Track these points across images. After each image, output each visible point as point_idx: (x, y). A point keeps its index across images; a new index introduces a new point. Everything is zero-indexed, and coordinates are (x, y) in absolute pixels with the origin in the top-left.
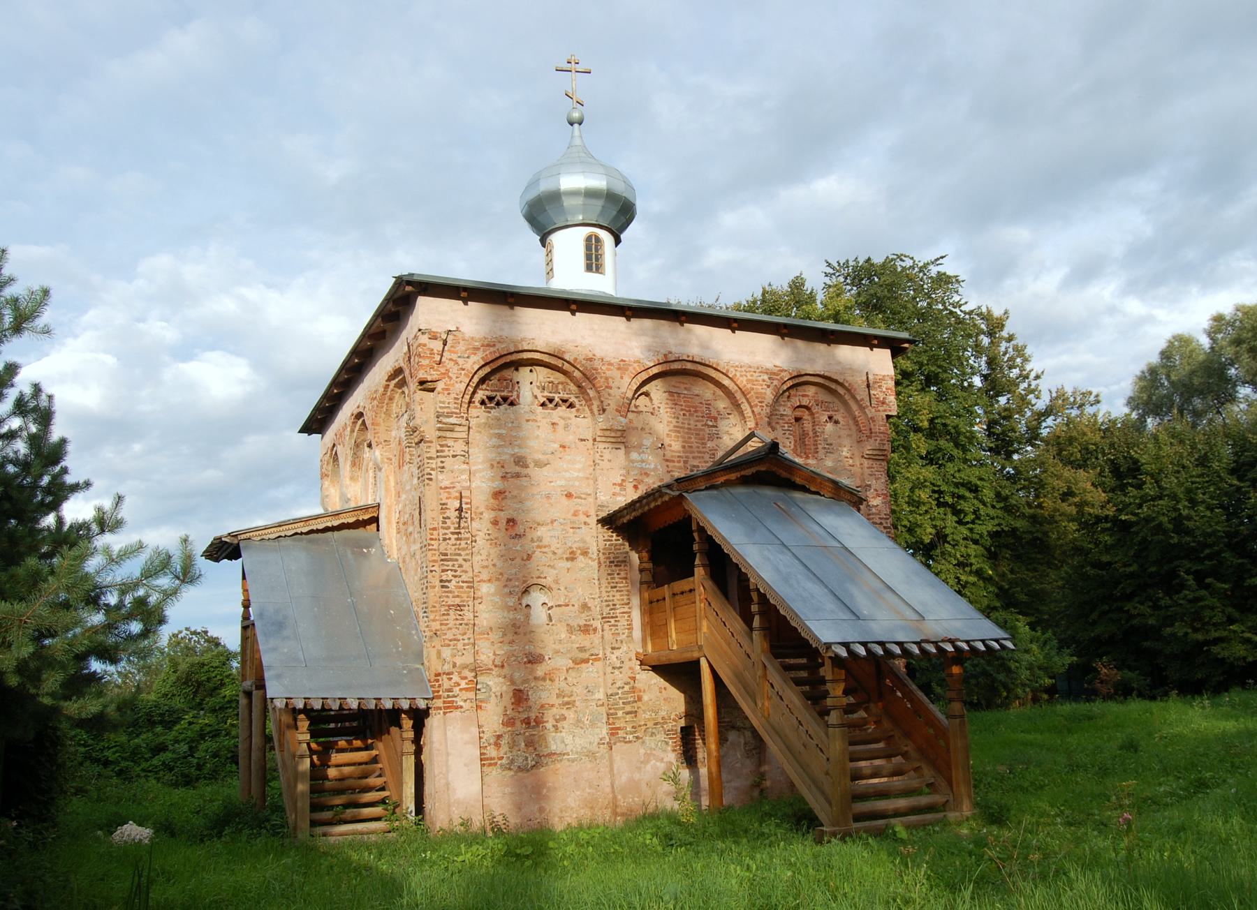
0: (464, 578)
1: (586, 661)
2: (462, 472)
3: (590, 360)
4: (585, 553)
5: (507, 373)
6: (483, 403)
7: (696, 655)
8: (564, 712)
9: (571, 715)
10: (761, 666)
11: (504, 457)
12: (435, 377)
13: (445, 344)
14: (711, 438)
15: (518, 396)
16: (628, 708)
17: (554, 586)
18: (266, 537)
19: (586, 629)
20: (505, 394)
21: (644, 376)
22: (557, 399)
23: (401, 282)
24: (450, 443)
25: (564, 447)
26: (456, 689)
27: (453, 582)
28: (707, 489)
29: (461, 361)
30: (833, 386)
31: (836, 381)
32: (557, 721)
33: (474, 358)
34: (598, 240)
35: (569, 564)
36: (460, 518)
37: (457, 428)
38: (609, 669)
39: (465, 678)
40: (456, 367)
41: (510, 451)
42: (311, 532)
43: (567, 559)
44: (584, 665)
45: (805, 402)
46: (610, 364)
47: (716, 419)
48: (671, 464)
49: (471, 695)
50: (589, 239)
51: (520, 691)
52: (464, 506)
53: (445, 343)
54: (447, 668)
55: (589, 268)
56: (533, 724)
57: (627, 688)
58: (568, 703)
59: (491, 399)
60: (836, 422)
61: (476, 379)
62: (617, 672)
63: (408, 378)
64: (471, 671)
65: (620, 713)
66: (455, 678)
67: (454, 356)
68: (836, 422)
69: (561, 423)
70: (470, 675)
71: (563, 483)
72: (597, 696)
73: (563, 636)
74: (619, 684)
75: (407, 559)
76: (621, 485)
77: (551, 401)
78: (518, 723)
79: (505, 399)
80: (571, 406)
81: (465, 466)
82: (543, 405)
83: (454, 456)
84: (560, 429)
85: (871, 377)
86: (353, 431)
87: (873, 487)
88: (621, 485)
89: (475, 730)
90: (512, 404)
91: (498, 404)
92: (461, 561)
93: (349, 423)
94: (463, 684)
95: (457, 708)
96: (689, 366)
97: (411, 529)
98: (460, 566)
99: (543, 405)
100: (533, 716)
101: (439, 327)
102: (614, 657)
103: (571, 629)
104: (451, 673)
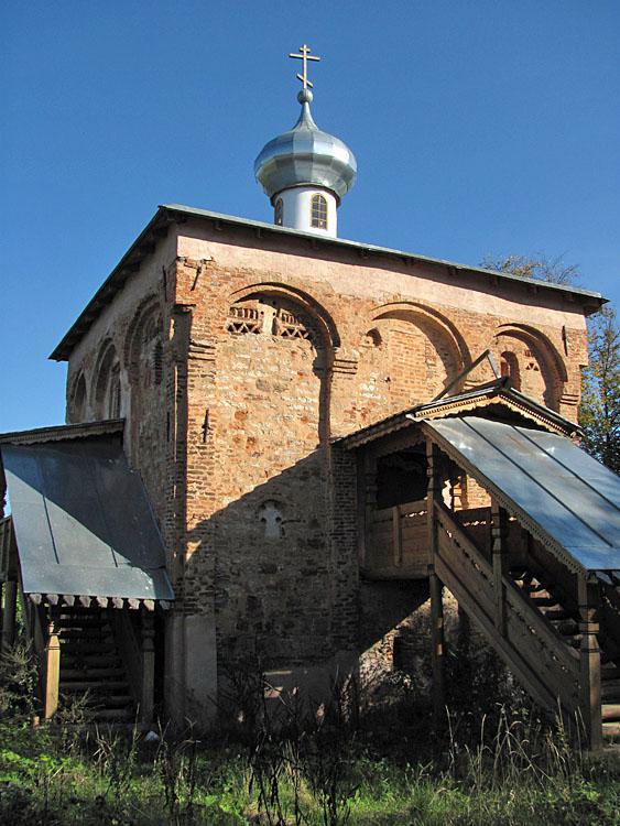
0: (208, 490)
1: (315, 573)
2: (208, 391)
3: (329, 296)
4: (316, 474)
6: (230, 329)
7: (425, 573)
8: (293, 619)
9: (299, 623)
10: (500, 585)
11: (249, 380)
12: (189, 302)
13: (199, 271)
14: (429, 376)
16: (350, 619)
17: (288, 502)
18: (24, 442)
19: (315, 544)
20: (250, 322)
22: (296, 331)
23: (164, 213)
24: (200, 363)
25: (301, 374)
26: (198, 593)
27: (198, 493)
28: (446, 417)
29: (213, 288)
32: (286, 627)
34: (324, 201)
35: (302, 483)
36: (205, 433)
37: (207, 351)
38: (334, 583)
39: (206, 584)
40: (209, 293)
41: (251, 374)
42: (64, 440)
43: (301, 479)
44: (312, 578)
45: (510, 349)
49: (210, 599)
50: (315, 199)
51: (253, 598)
52: (210, 423)
53: (199, 271)
54: (188, 573)
55: (315, 224)
56: (264, 629)
57: (350, 600)
58: (297, 611)
59: (238, 326)
62: (342, 585)
63: (163, 303)
64: (211, 577)
65: (344, 623)
66: (196, 583)
67: (208, 284)
69: (300, 352)
70: (210, 581)
71: (301, 407)
72: (322, 606)
73: (294, 549)
74: (344, 596)
75: (150, 470)
76: (351, 413)
77: (291, 331)
78: (251, 628)
79: (250, 327)
81: (210, 386)
82: (284, 334)
83: (203, 376)
84: (298, 357)
85: (567, 330)
86: (100, 356)
88: (351, 413)
89: (213, 632)
90: (256, 332)
91: (244, 331)
92: (205, 475)
93: (98, 348)
94: (203, 590)
95: (197, 611)
97: (155, 443)
98: (205, 479)
99: (284, 334)
100: (264, 622)
101: (196, 257)
102: (340, 571)
103: (301, 543)
104: (194, 578)
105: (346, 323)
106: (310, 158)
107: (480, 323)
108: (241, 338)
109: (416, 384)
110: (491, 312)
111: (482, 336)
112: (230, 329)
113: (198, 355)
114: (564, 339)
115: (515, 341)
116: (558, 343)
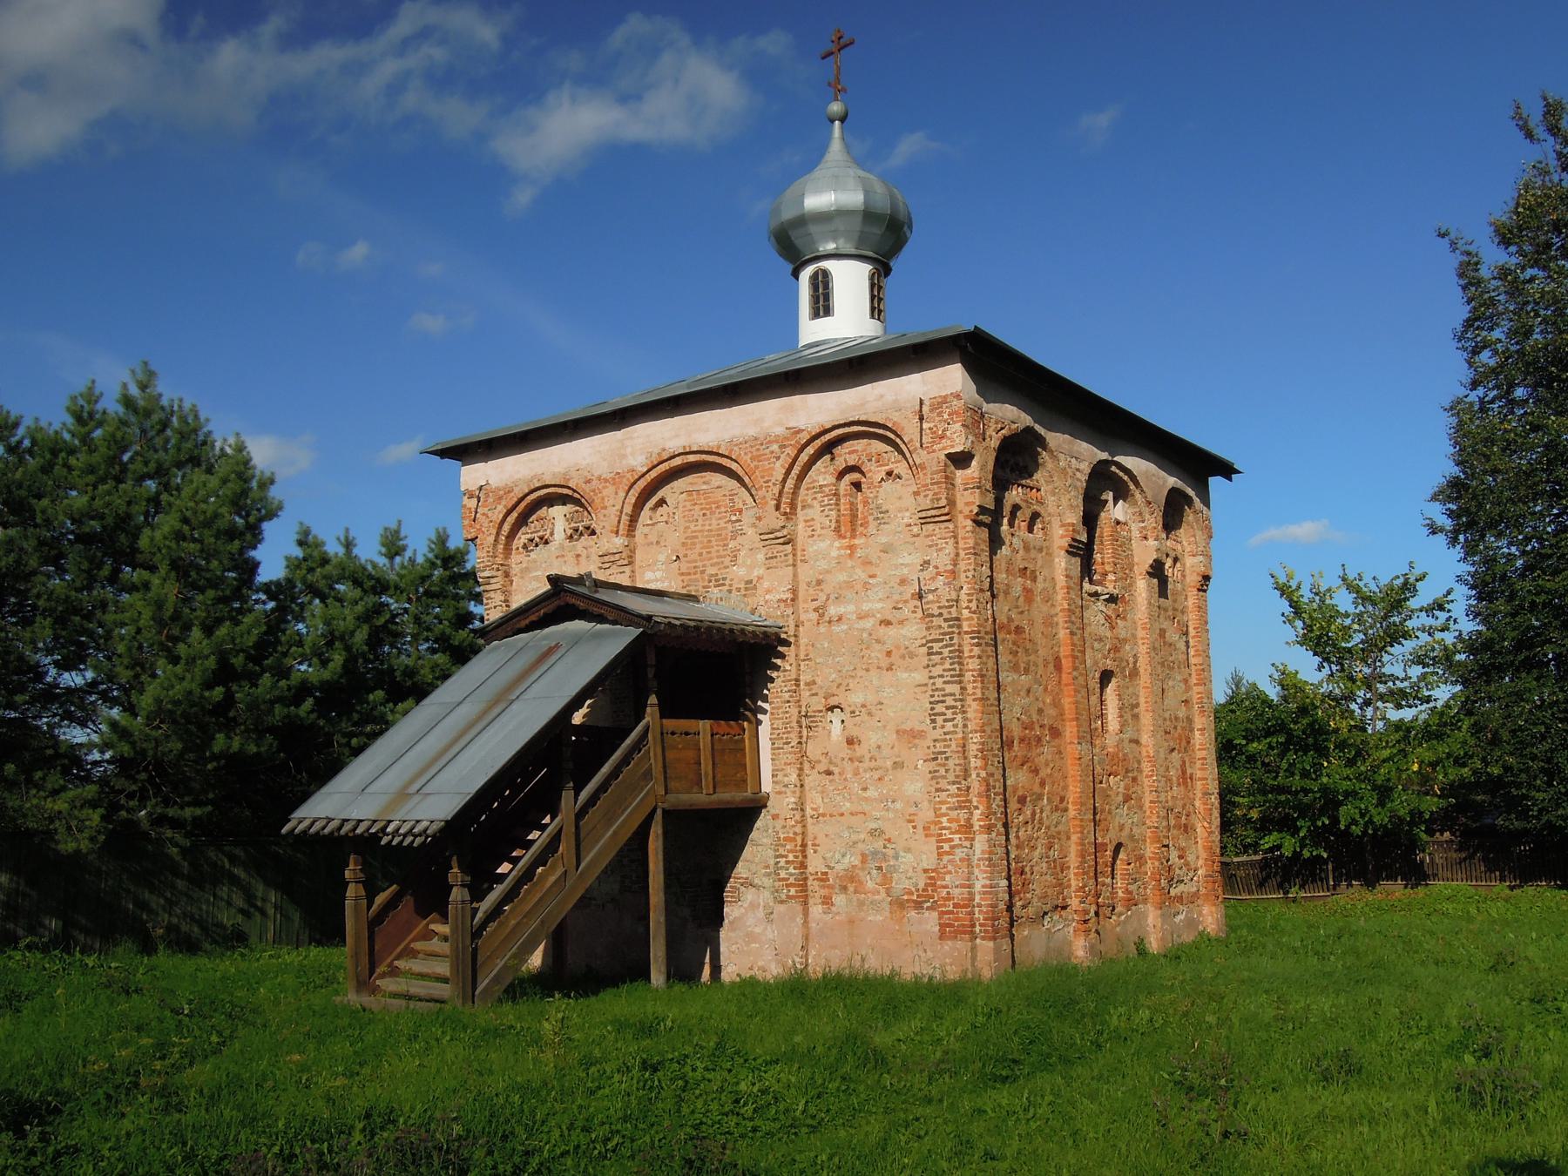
3: (588, 481)
5: (543, 512)
14: (734, 538)
15: (552, 534)
21: (642, 484)
24: (492, 594)
33: (500, 507)
46: (606, 481)
47: (741, 511)
48: (686, 578)
50: (814, 277)
61: (506, 527)
77: (576, 530)
79: (541, 538)
80: (593, 533)
82: (571, 537)
84: (583, 559)
85: (927, 403)
87: (933, 563)
90: (546, 542)
96: (692, 458)
101: (473, 487)
105: (605, 508)
106: (803, 221)
107: (775, 447)
109: (714, 554)
111: (778, 464)
112: (525, 547)
113: (488, 587)
114: (921, 419)
115: (860, 444)
116: (910, 431)
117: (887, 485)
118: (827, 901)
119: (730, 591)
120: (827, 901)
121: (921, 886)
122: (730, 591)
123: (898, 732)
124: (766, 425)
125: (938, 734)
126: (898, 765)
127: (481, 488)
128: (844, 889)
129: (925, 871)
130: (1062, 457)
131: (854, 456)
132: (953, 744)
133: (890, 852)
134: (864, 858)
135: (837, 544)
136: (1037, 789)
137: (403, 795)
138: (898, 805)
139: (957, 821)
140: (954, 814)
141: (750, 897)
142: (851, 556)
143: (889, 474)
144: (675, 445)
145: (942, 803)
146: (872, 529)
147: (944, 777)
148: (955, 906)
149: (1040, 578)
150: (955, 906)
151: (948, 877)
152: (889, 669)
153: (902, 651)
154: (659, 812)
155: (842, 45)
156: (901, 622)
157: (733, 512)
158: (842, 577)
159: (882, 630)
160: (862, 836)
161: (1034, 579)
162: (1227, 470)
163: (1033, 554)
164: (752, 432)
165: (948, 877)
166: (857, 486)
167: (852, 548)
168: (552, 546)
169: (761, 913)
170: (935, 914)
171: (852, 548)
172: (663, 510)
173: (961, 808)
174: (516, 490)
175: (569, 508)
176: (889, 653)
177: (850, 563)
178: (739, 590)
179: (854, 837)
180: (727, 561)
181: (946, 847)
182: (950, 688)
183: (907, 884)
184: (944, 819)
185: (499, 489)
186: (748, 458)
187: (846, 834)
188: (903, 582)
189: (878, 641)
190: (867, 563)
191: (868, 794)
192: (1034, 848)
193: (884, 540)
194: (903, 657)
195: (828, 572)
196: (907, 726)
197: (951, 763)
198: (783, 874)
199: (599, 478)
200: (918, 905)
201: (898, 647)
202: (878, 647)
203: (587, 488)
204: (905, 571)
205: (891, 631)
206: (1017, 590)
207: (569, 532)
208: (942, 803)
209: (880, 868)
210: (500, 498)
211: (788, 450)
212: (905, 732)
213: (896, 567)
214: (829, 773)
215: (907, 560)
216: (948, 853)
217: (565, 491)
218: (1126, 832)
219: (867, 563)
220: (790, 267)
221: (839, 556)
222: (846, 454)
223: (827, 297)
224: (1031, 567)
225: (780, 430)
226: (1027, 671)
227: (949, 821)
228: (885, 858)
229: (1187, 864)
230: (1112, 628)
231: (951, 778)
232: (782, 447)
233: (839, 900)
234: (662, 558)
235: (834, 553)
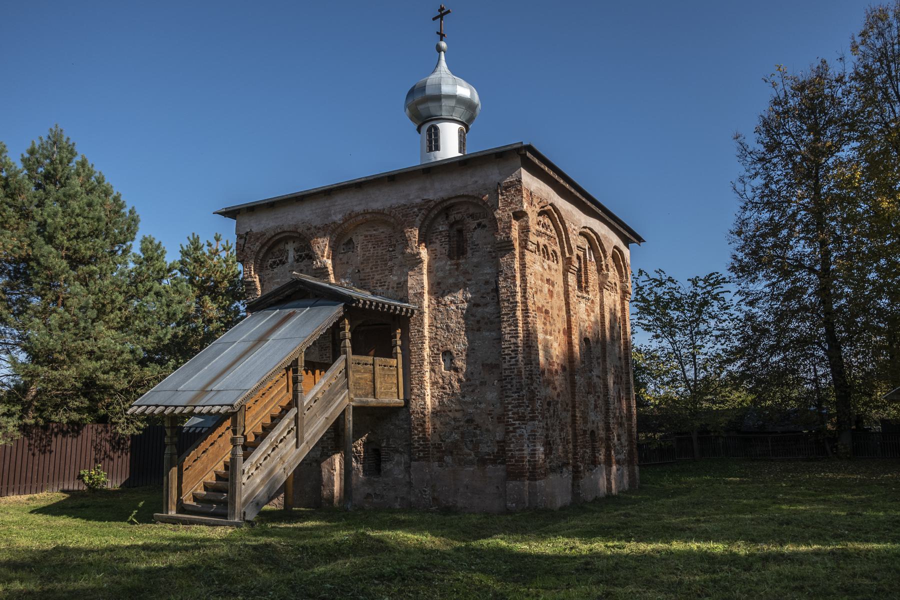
3: (309, 229)
5: (281, 246)
14: (391, 260)
15: (287, 258)
30: (475, 201)
31: (474, 197)
33: (257, 244)
45: (458, 217)
46: (319, 228)
47: (395, 246)
50: (429, 130)
59: (274, 262)
60: (484, 226)
61: (261, 255)
68: (484, 226)
77: (300, 256)
79: (280, 261)
90: (284, 263)
99: (297, 261)
107: (416, 209)
108: (275, 270)
110: (425, 197)
112: (271, 266)
117: (478, 231)
118: (441, 459)
119: (388, 289)
120: (441, 459)
121: (496, 450)
122: (388, 289)
123: (483, 365)
124: (411, 197)
125: (505, 366)
126: (483, 383)
127: (247, 233)
128: (451, 453)
129: (498, 442)
130: (566, 222)
131: (459, 215)
132: (516, 371)
133: (478, 432)
134: (463, 434)
135: (449, 263)
136: (556, 398)
137: (204, 391)
138: (483, 406)
139: (518, 413)
140: (515, 410)
141: (396, 459)
142: (457, 269)
143: (479, 225)
144: (358, 209)
145: (509, 403)
146: (469, 254)
147: (510, 389)
148: (516, 461)
149: (556, 286)
150: (516, 461)
151: (512, 445)
152: (479, 330)
153: (486, 320)
154: (351, 408)
155: (442, 14)
156: (486, 305)
157: (391, 246)
158: (451, 281)
159: (474, 309)
160: (462, 423)
161: (553, 286)
162: (640, 240)
163: (553, 272)
164: (403, 202)
165: (512, 445)
166: (460, 231)
167: (458, 265)
168: (287, 266)
169: (402, 467)
170: (503, 467)
171: (458, 265)
172: (351, 246)
173: (521, 406)
174: (267, 234)
175: (296, 245)
176: (478, 322)
177: (456, 273)
178: (393, 288)
179: (457, 424)
180: (387, 272)
181: (511, 429)
182: (513, 340)
183: (487, 450)
184: (510, 413)
185: (257, 233)
186: (400, 216)
187: (453, 423)
188: (487, 282)
189: (472, 315)
190: (466, 273)
191: (466, 399)
192: (554, 431)
193: (475, 260)
194: (486, 323)
195: (444, 278)
196: (489, 362)
197: (514, 381)
198: (416, 445)
199: (315, 227)
200: (494, 462)
201: (483, 318)
202: (472, 318)
203: (308, 232)
204: (488, 277)
205: (480, 309)
206: (546, 290)
207: (297, 257)
208: (509, 403)
209: (472, 441)
210: (258, 239)
211: (423, 211)
212: (487, 365)
213: (483, 274)
214: (444, 388)
215: (489, 271)
216: (512, 432)
217: (295, 235)
218: (595, 425)
219: (466, 273)
220: (416, 127)
221: (450, 270)
222: (454, 216)
223: (437, 140)
224: (552, 279)
225: (418, 201)
226: (551, 334)
227: (513, 414)
228: (475, 435)
229: (621, 444)
230: (588, 316)
231: (514, 389)
232: (420, 210)
233: (448, 459)
234: (349, 271)
235: (447, 268)
